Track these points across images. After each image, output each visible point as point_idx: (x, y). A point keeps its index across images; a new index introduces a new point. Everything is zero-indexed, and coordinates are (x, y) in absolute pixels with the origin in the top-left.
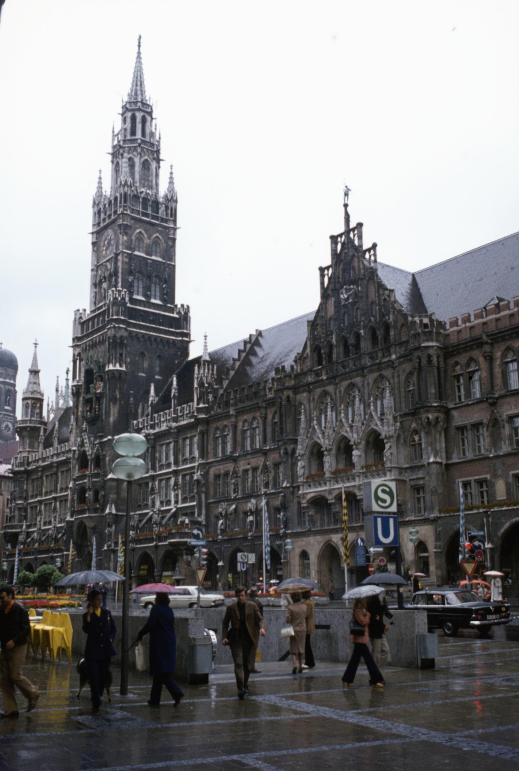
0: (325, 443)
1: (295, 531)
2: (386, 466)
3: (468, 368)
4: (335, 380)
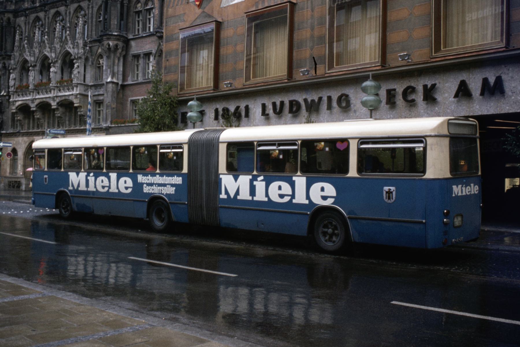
2: (73, 82)
3: (147, 6)
4: (45, 7)
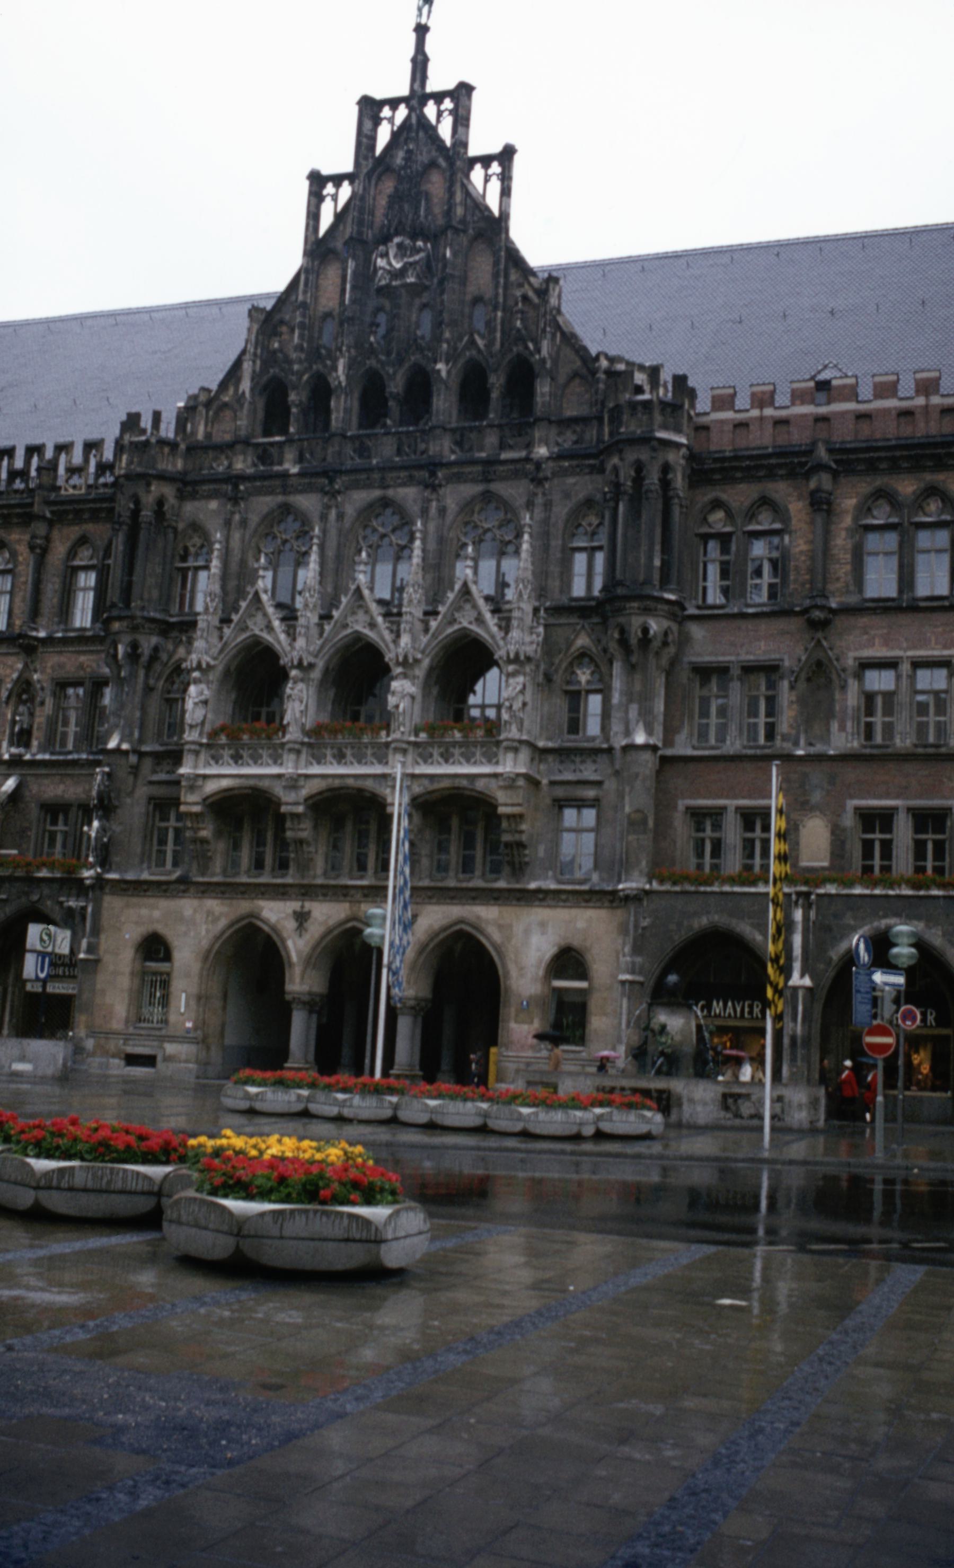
0: (300, 647)
1: (130, 876)
4: (332, 481)
